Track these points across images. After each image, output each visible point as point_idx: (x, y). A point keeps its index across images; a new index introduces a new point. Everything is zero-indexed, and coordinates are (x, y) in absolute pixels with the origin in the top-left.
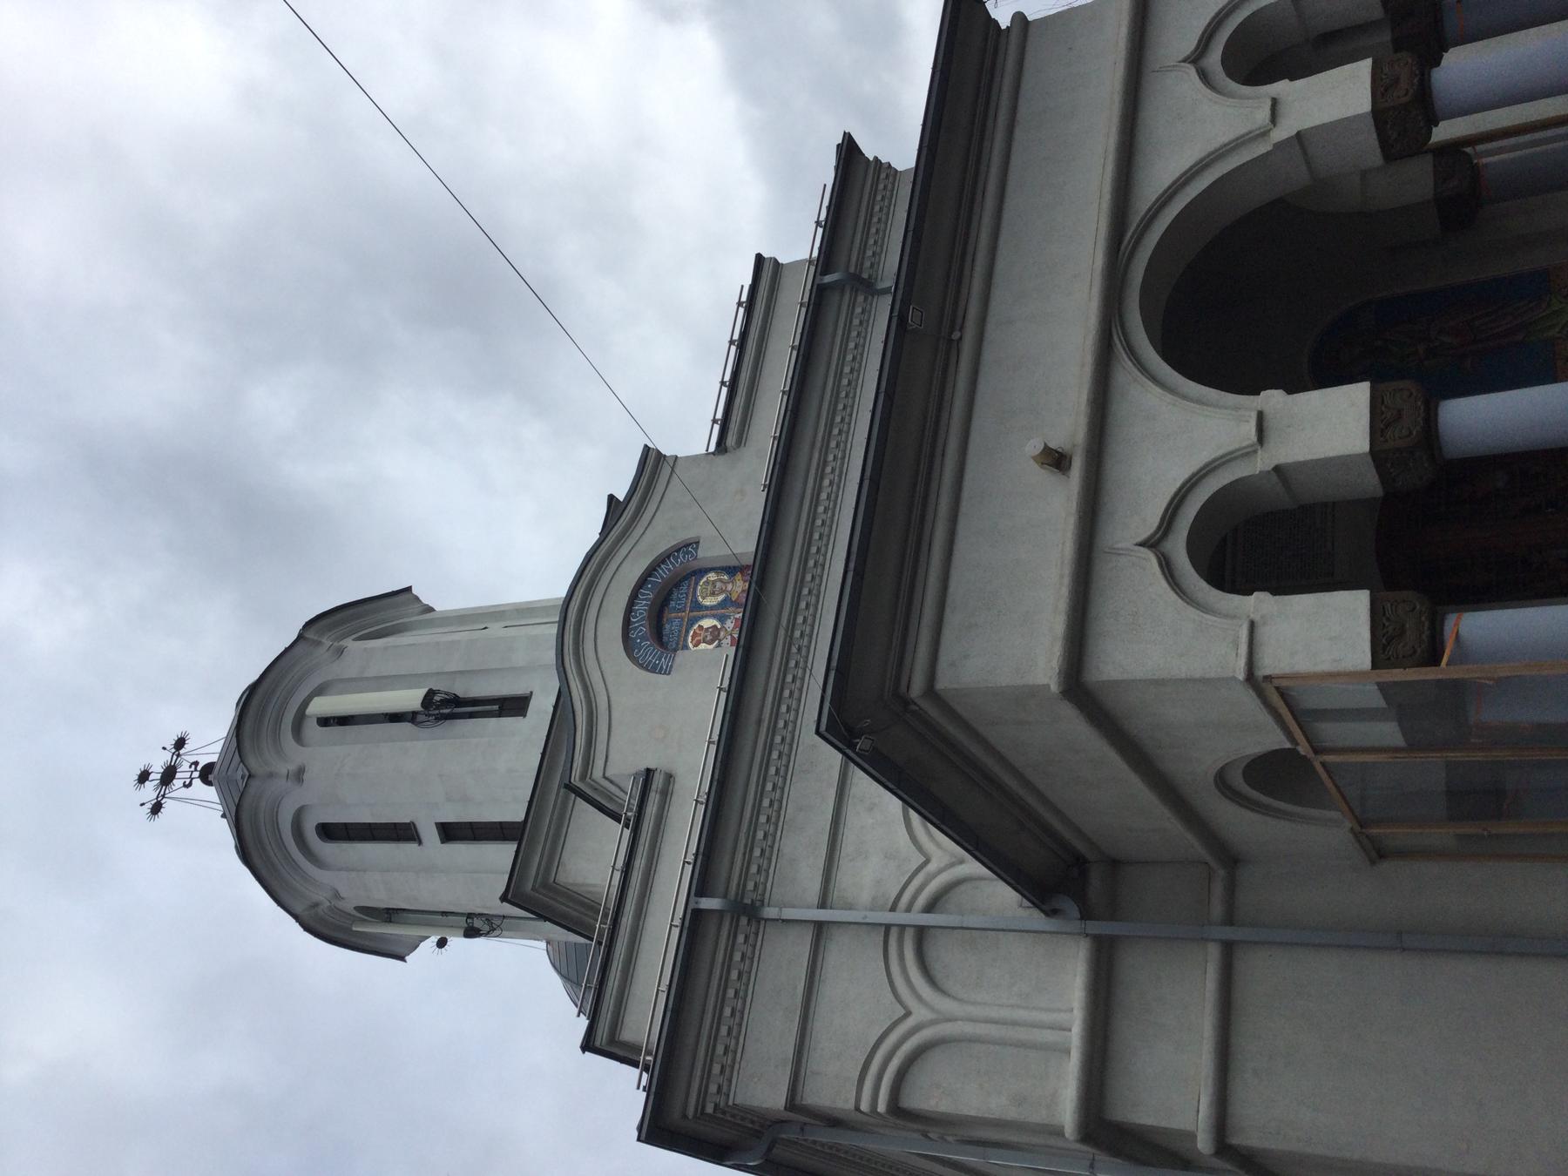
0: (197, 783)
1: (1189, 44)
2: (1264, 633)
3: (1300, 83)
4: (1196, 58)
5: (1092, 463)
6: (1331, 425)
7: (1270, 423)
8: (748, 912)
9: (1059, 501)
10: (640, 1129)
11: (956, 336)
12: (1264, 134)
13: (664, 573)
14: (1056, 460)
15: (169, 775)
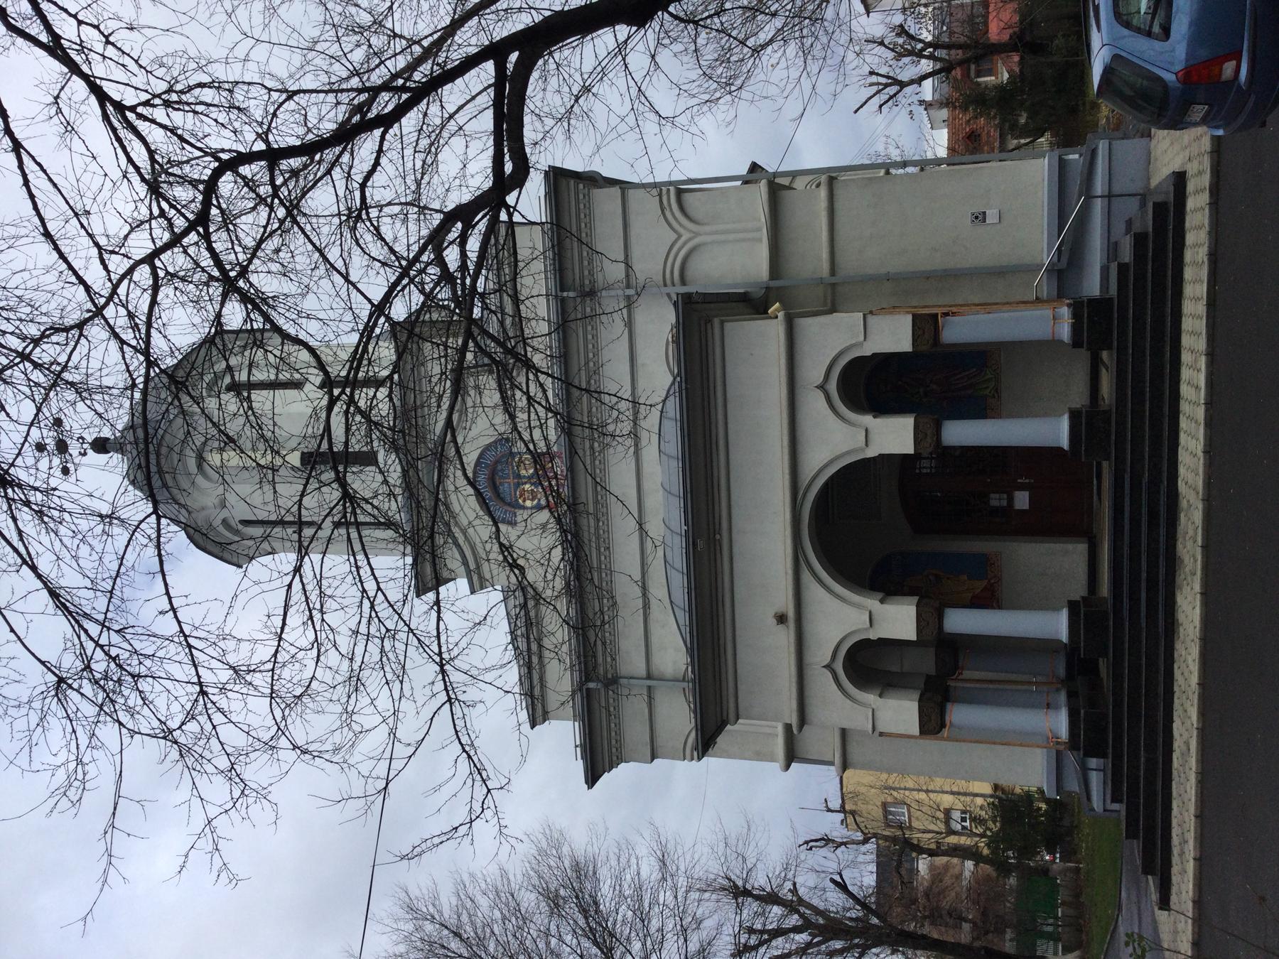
0: (90, 452)
1: (818, 376)
2: (878, 714)
3: (878, 420)
4: (822, 387)
5: (796, 619)
6: (899, 620)
7: (875, 617)
8: (612, 682)
9: (784, 638)
10: (587, 782)
11: (718, 537)
12: (862, 450)
13: (490, 458)
14: (781, 619)
15: (62, 447)
